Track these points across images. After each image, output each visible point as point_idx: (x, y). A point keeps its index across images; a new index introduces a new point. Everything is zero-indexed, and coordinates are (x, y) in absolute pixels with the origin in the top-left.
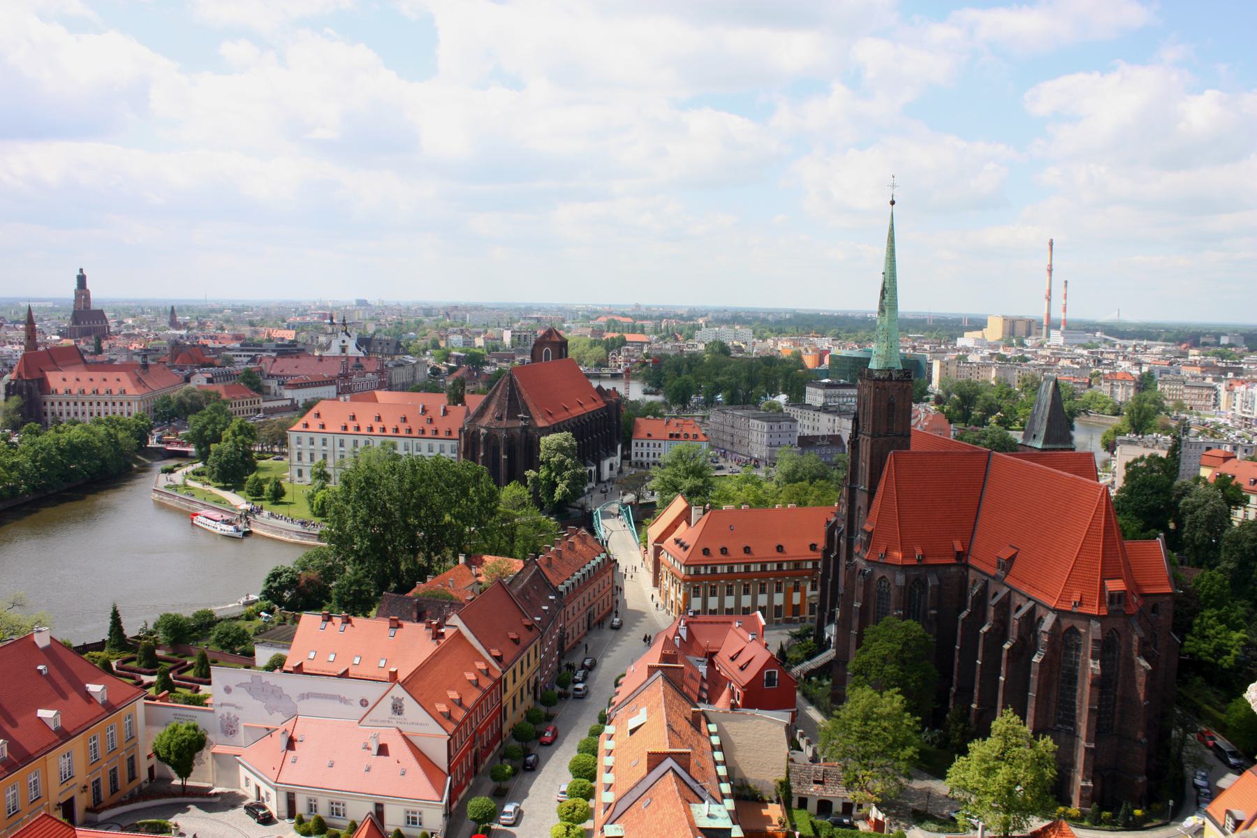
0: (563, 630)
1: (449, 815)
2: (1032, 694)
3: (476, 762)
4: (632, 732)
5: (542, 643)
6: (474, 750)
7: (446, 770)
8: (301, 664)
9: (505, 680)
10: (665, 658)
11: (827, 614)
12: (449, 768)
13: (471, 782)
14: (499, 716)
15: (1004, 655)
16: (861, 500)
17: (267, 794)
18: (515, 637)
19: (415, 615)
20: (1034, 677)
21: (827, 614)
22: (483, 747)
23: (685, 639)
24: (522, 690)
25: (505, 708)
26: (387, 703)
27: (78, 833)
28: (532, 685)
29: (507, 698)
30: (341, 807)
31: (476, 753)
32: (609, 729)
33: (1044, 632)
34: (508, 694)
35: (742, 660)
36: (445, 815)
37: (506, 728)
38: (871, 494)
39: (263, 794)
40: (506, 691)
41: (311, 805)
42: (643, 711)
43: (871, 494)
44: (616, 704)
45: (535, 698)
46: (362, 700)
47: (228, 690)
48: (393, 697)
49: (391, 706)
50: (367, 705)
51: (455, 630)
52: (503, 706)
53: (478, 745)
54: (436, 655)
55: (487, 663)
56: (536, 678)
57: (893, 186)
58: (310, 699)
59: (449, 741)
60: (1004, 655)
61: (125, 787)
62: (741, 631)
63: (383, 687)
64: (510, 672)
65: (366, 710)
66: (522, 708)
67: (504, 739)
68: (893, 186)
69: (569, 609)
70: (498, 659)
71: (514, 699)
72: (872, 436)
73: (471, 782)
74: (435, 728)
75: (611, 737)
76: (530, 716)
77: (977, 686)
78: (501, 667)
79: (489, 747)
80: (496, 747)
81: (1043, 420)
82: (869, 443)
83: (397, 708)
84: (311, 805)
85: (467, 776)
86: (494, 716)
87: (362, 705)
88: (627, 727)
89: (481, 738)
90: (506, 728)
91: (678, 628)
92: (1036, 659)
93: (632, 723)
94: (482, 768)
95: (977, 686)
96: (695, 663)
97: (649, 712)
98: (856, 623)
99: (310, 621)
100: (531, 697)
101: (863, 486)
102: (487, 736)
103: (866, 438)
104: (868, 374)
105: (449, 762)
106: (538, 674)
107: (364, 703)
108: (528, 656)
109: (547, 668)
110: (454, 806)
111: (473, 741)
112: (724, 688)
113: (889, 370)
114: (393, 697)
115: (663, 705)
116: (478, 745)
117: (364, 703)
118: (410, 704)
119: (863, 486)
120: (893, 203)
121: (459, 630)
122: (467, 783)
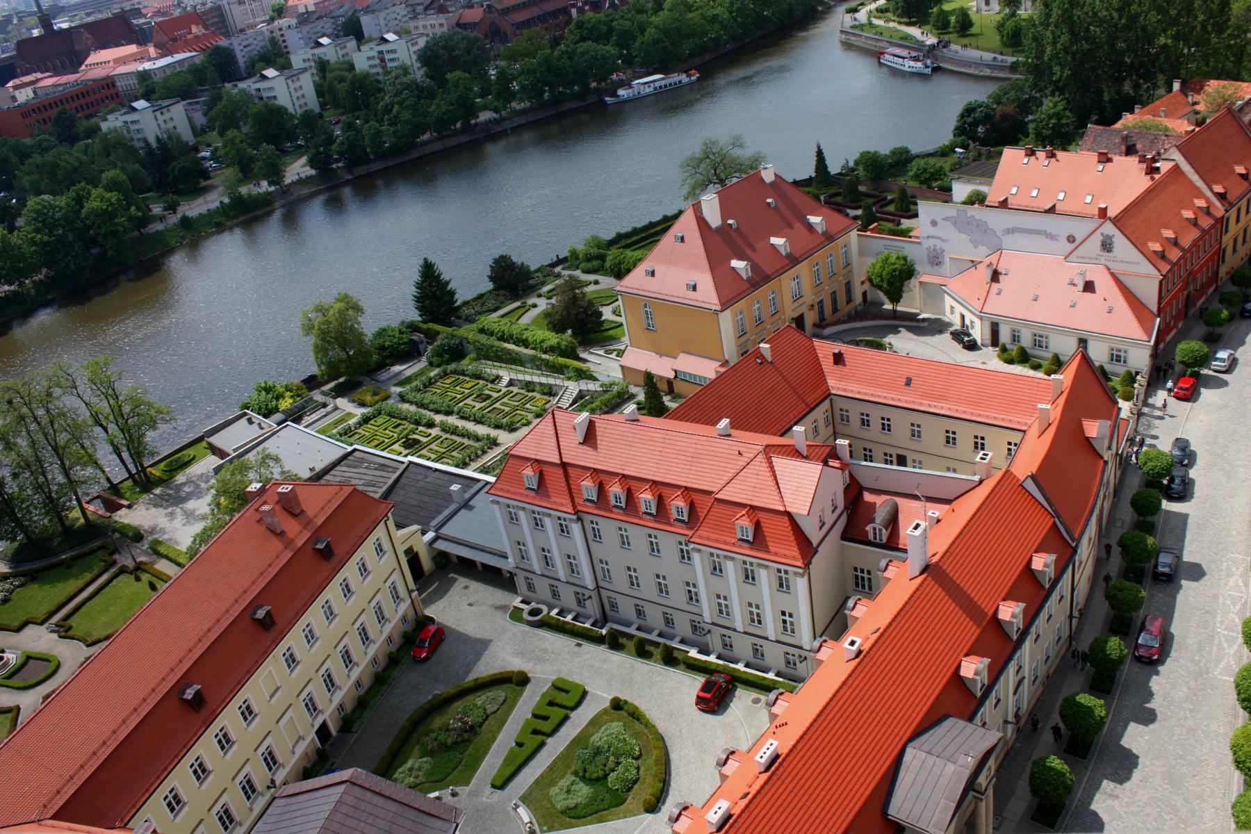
1: (1154, 356)
3: (1188, 304)
6: (1186, 292)
7: (1155, 310)
8: (1006, 200)
9: (1228, 220)
12: (1159, 309)
13: (1180, 325)
14: (1216, 257)
17: (972, 322)
19: (1123, 148)
22: (1195, 290)
25: (1224, 250)
26: (1097, 239)
27: (815, 343)
29: (1227, 239)
30: (1044, 339)
31: (1188, 295)
34: (1230, 234)
36: (1151, 356)
37: (1223, 271)
39: (967, 322)
40: (1227, 231)
41: (1014, 336)
46: (1069, 237)
47: (934, 223)
48: (1102, 234)
49: (1100, 243)
50: (1074, 241)
51: (1171, 164)
53: (1191, 288)
54: (1151, 191)
55: (1208, 200)
58: (1016, 234)
59: (1161, 282)
65: (1073, 246)
67: (1219, 284)
70: (1221, 197)
71: (1235, 240)
73: (1180, 325)
74: (1146, 268)
78: (1223, 205)
79: (1204, 288)
80: (1210, 291)
83: (1107, 246)
84: (1014, 336)
85: (1177, 318)
86: (1211, 258)
87: (1069, 241)
89: (1195, 279)
90: (1223, 271)
94: (1192, 312)
99: (1012, 157)
102: (1201, 278)
105: (1159, 303)
107: (1071, 239)
110: (1161, 346)
111: (1186, 284)
114: (1102, 234)
116: (1191, 288)
117: (1071, 239)
118: (1120, 241)
122: (1175, 326)
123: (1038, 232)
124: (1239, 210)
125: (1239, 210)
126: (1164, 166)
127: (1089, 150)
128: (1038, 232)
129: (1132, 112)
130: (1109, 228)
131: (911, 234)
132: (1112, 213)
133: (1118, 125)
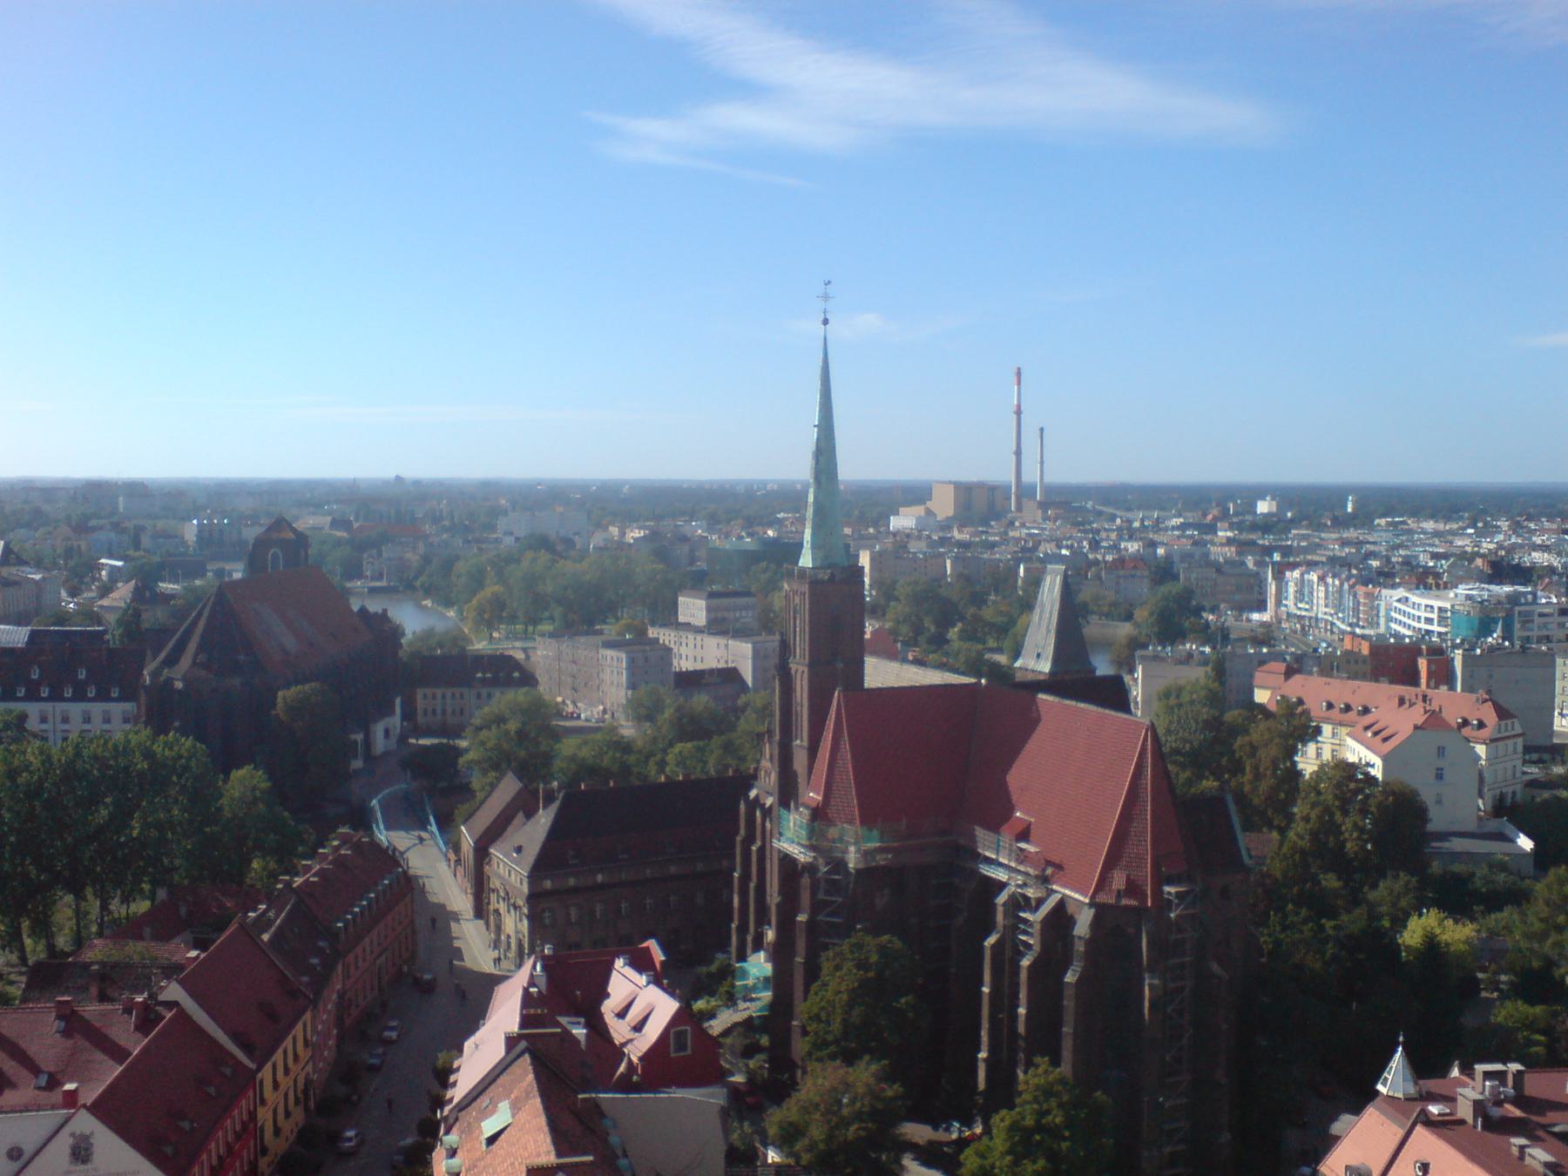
2: (1067, 1029)
4: (492, 1140)
5: (314, 1018)
9: (261, 1082)
10: (525, 1021)
11: (749, 938)
15: (1023, 976)
16: (800, 761)
20: (1069, 1003)
21: (749, 938)
23: (544, 992)
24: (286, 1095)
28: (301, 1086)
32: (451, 1139)
33: (1080, 938)
35: (634, 1014)
38: (813, 750)
42: (504, 1107)
43: (813, 750)
44: (455, 1101)
45: (307, 1109)
52: (259, 1125)
56: (308, 1074)
57: (826, 297)
60: (1023, 976)
62: (630, 972)
66: (287, 1126)
68: (826, 297)
69: (351, 957)
72: (811, 666)
75: (452, 1153)
76: (305, 1136)
77: (985, 1025)
81: (1048, 631)
82: (806, 675)
88: (481, 1132)
91: (532, 975)
92: (1070, 977)
93: (489, 1127)
95: (985, 1025)
96: (569, 1027)
97: (515, 1108)
98: (801, 944)
101: (800, 743)
103: (801, 669)
104: (799, 573)
106: (309, 1068)
112: (622, 1060)
113: (830, 566)
115: (535, 1092)
119: (800, 743)
120: (826, 322)
124: (274, 1067)
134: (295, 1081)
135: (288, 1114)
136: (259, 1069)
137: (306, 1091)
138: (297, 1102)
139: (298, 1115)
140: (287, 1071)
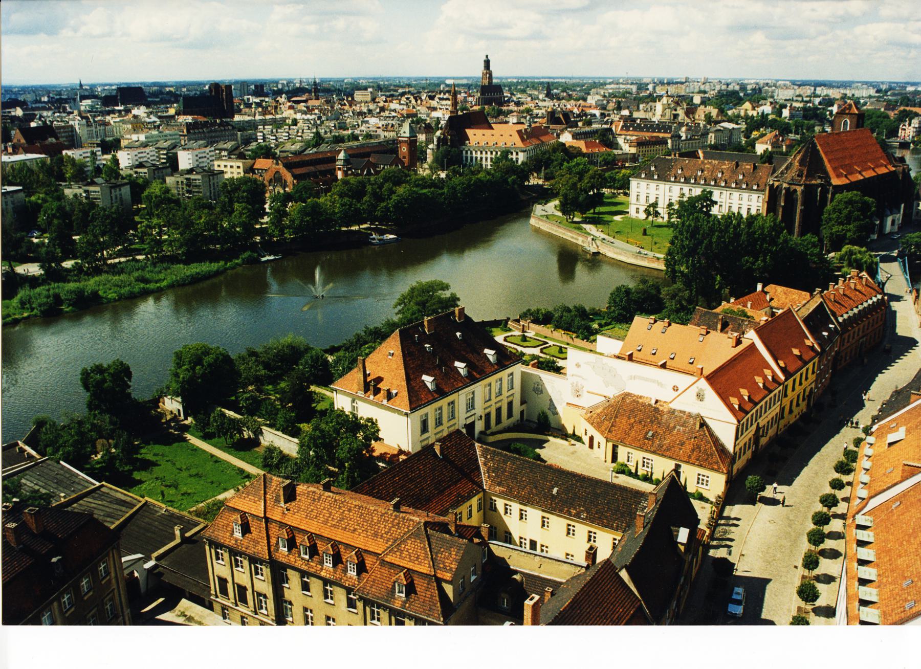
0: (837, 353)
5: (819, 362)
8: (632, 354)
18: (798, 354)
19: (719, 327)
24: (798, 396)
28: (807, 393)
45: (808, 405)
47: (578, 365)
51: (751, 342)
55: (773, 372)
56: (812, 388)
61: (506, 422)
63: (694, 379)
64: (790, 381)
66: (796, 411)
70: (783, 370)
71: (791, 402)
99: (640, 322)
100: (805, 402)
106: (813, 385)
108: (807, 370)
109: (821, 382)
121: (753, 343)
123: (653, 381)
124: (794, 380)
125: (794, 380)
126: (745, 343)
127: (695, 325)
128: (653, 381)
129: (728, 302)
130: (703, 384)
131: (562, 371)
132: (707, 372)
133: (718, 310)
134: (804, 390)
135: (798, 405)
136: (786, 380)
137: (809, 396)
138: (804, 399)
139: (803, 405)
140: (801, 384)
